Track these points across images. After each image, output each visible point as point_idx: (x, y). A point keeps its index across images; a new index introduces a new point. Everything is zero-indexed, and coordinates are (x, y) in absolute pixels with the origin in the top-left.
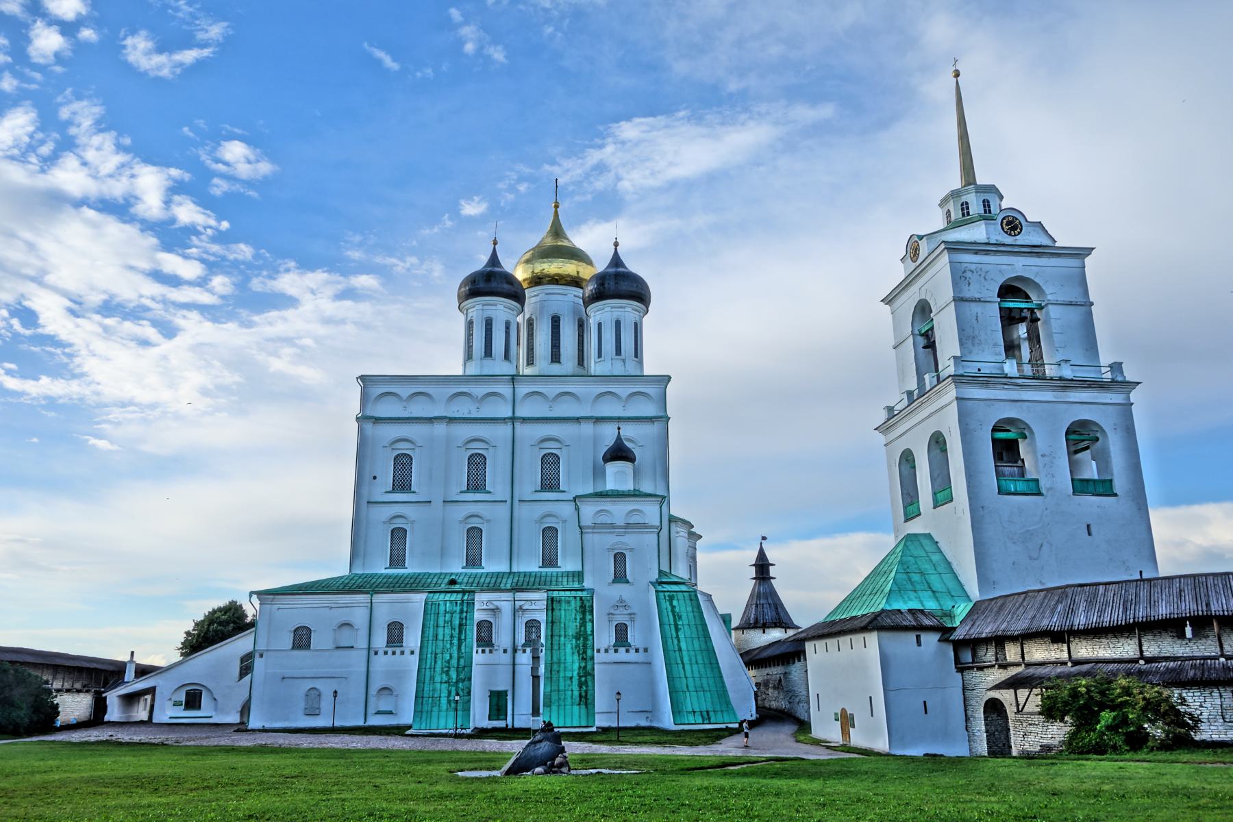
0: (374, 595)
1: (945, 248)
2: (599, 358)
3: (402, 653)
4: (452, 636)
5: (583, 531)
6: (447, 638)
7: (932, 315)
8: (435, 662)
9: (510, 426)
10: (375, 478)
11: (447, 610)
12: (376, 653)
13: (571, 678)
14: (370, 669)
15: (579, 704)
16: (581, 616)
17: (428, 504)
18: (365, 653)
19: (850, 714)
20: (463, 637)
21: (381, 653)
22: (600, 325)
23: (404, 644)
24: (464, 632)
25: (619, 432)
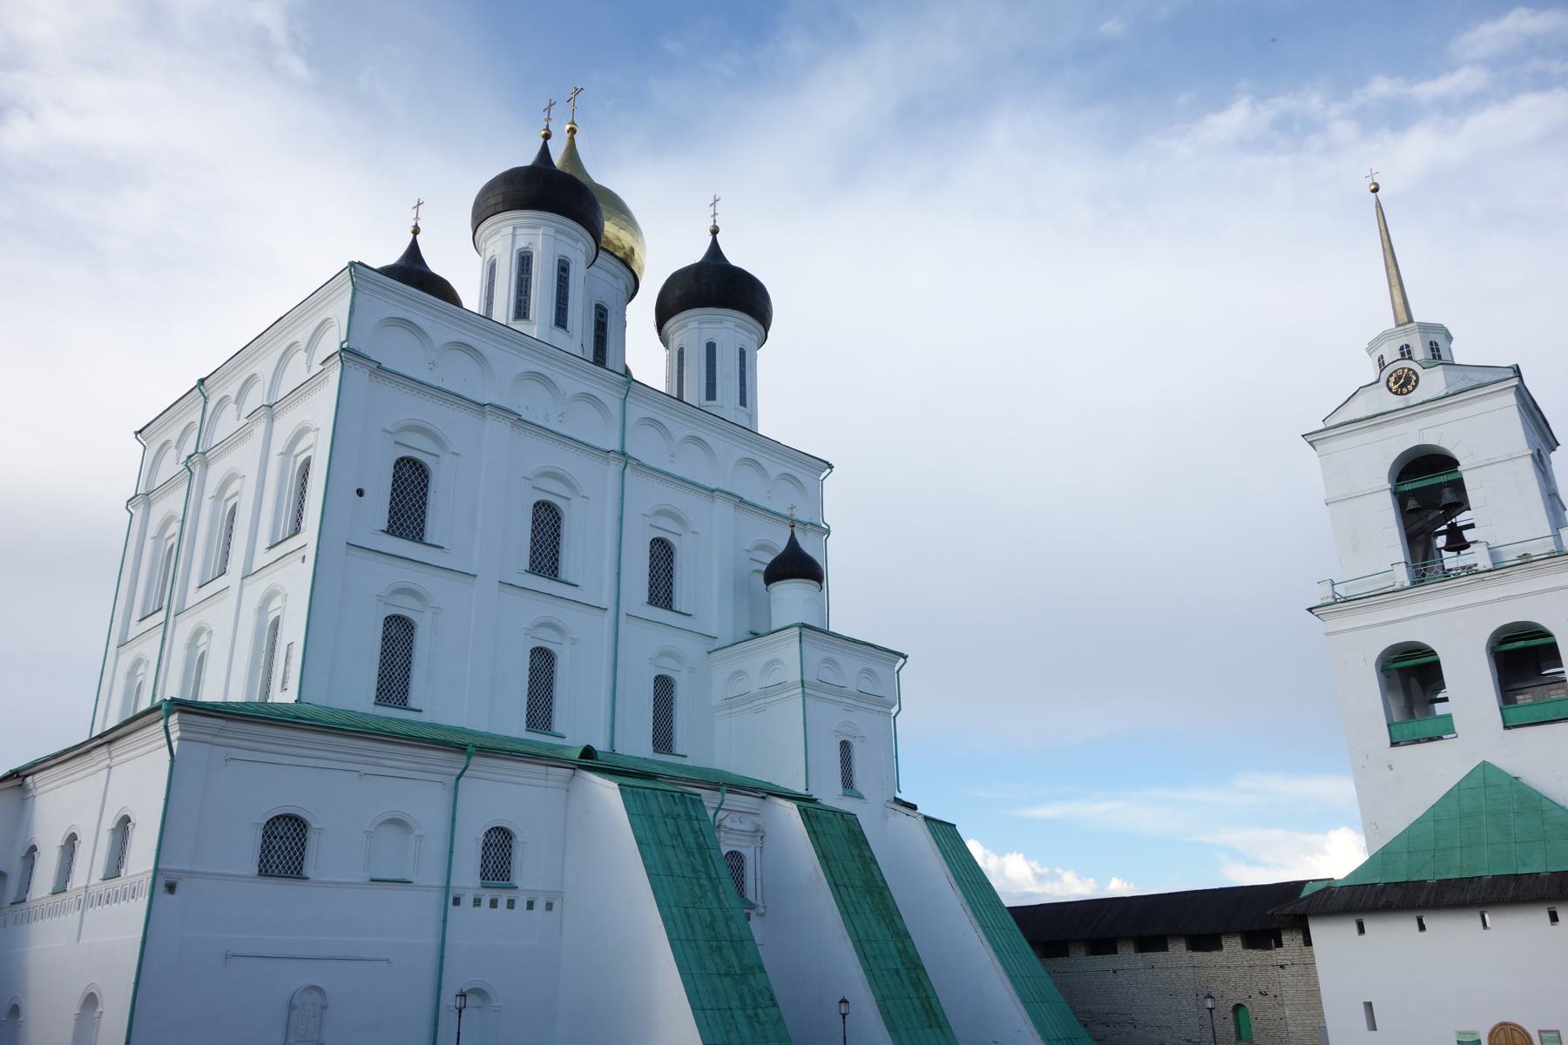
0: (475, 759)
1: (1516, 386)
2: (708, 399)
3: (511, 904)
4: (694, 870)
5: (806, 690)
6: (689, 873)
7: (1459, 468)
8: (692, 927)
9: (614, 468)
10: (360, 493)
11: (665, 811)
12: (457, 901)
13: (897, 971)
14: (447, 941)
15: (930, 1027)
16: (855, 852)
17: (470, 579)
18: (434, 900)
19: (1540, 1032)
20: (714, 875)
21: (467, 901)
22: (711, 349)
23: (516, 879)
24: (709, 861)
25: (793, 534)
